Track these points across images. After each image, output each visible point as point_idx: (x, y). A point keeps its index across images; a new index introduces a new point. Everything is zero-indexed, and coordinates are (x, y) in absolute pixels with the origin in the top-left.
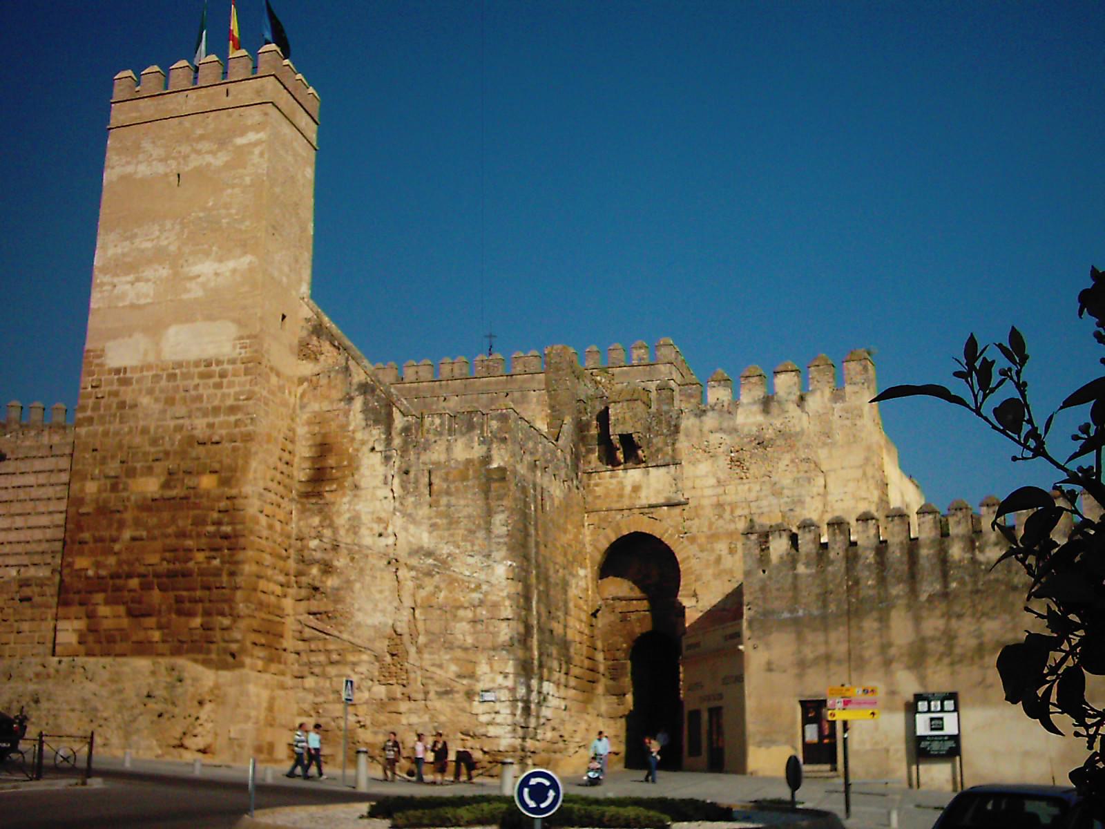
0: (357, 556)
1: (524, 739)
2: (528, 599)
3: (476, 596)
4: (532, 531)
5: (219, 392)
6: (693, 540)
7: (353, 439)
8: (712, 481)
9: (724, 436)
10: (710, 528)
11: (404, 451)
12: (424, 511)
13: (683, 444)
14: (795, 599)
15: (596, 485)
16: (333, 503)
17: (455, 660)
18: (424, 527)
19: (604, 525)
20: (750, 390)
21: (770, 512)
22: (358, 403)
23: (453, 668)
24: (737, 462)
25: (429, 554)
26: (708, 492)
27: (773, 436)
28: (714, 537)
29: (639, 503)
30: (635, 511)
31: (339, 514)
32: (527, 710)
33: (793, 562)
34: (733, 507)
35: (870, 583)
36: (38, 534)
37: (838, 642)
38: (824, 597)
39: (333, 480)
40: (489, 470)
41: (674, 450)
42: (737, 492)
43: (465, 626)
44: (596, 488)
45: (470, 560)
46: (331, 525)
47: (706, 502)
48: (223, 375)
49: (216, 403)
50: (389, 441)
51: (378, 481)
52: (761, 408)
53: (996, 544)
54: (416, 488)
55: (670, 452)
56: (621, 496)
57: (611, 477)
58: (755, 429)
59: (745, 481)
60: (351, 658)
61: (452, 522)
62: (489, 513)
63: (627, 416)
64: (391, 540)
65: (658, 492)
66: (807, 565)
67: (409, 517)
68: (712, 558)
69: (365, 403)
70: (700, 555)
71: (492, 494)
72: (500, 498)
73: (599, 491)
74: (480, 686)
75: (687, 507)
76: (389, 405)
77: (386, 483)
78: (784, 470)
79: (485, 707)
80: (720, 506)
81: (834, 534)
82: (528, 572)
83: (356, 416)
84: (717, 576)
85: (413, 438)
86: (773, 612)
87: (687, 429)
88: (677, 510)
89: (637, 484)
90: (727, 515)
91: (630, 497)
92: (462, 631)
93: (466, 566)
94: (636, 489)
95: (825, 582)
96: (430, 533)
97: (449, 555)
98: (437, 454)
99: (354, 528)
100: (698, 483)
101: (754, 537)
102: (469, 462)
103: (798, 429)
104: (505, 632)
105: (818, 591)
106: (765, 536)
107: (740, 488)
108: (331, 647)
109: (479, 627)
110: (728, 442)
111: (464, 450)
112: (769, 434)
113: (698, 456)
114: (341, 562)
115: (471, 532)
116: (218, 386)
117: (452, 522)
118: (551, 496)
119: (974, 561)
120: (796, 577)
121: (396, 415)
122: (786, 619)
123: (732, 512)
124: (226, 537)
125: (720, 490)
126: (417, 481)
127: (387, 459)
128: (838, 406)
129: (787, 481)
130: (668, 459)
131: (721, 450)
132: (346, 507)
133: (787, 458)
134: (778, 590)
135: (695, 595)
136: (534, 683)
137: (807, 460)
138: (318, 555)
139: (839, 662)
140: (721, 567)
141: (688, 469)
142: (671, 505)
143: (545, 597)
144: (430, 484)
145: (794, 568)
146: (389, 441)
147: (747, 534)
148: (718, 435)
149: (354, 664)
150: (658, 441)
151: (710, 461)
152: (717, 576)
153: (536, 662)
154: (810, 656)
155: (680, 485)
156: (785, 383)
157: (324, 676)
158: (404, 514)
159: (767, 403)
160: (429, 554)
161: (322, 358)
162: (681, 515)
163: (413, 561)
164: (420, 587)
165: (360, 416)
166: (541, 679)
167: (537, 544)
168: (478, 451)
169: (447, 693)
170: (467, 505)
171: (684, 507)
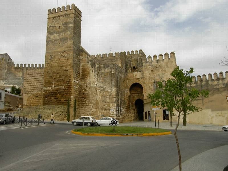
0: (90, 88)
1: (118, 117)
2: (118, 94)
3: (110, 94)
4: (119, 83)
5: (67, 62)
6: (145, 84)
7: (89, 69)
8: (148, 74)
11: (97, 71)
12: (101, 80)
13: (143, 68)
16: (86, 80)
17: (107, 104)
18: (101, 83)
21: (158, 79)
22: (90, 63)
23: (106, 106)
24: (152, 71)
25: (102, 87)
26: (148, 76)
28: (149, 83)
31: (87, 81)
32: (118, 112)
34: (152, 78)
36: (39, 86)
39: (86, 76)
40: (111, 74)
42: (153, 76)
43: (108, 99)
45: (109, 88)
46: (86, 83)
47: (148, 77)
48: (68, 59)
49: (67, 64)
50: (95, 69)
51: (93, 76)
53: (194, 84)
54: (100, 77)
56: (133, 77)
60: (90, 104)
61: (106, 82)
62: (111, 80)
64: (96, 85)
67: (98, 81)
69: (91, 63)
71: (112, 78)
72: (113, 78)
73: (130, 76)
74: (111, 108)
76: (95, 63)
77: (95, 76)
78: (160, 72)
79: (111, 112)
80: (150, 78)
82: (118, 90)
83: (90, 66)
84: (149, 90)
85: (99, 69)
88: (143, 79)
92: (108, 100)
93: (108, 89)
94: (136, 75)
96: (102, 84)
97: (105, 87)
98: (103, 71)
99: (90, 84)
100: (146, 74)
101: (155, 83)
102: (108, 72)
104: (115, 100)
108: (87, 103)
109: (110, 99)
111: (107, 70)
112: (158, 66)
114: (88, 89)
115: (108, 83)
116: (67, 61)
117: (106, 82)
118: (122, 77)
119: (191, 86)
121: (96, 65)
123: (152, 79)
124: (69, 86)
125: (150, 75)
126: (100, 75)
127: (95, 72)
128: (169, 61)
129: (161, 74)
133: (161, 70)
136: (120, 108)
137: (164, 70)
138: (84, 88)
142: (142, 78)
143: (121, 94)
144: (102, 76)
146: (95, 69)
147: (154, 82)
149: (90, 105)
150: (140, 68)
152: (149, 90)
153: (120, 105)
157: (86, 107)
158: (98, 81)
160: (102, 87)
161: (84, 56)
163: (99, 89)
164: (101, 93)
165: (90, 65)
166: (121, 107)
167: (119, 85)
168: (109, 70)
169: (105, 110)
170: (108, 79)
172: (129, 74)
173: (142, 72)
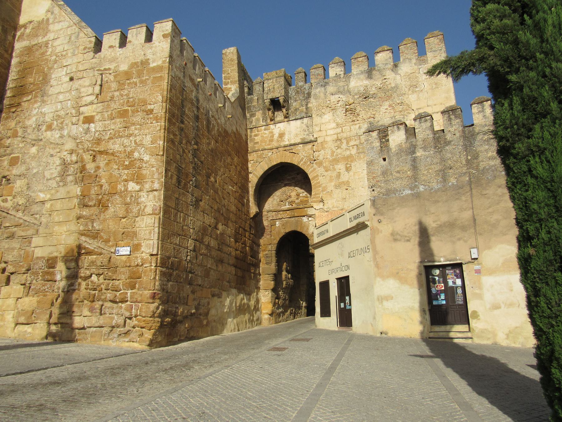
8: (334, 125)
9: (341, 96)
10: (332, 155)
13: (313, 103)
14: (415, 178)
15: (256, 135)
19: (260, 160)
20: (358, 66)
27: (376, 92)
28: (336, 161)
29: (282, 144)
30: (280, 149)
31: (29, 117)
33: (412, 149)
34: (348, 140)
35: (490, 154)
37: (462, 210)
38: (443, 174)
41: (307, 108)
44: (256, 138)
47: (328, 139)
52: (367, 75)
55: (305, 110)
57: (265, 130)
58: (362, 89)
59: (356, 122)
63: (276, 87)
65: (297, 135)
66: (425, 148)
68: (334, 174)
70: (326, 174)
73: (257, 139)
75: (315, 144)
80: (338, 139)
81: (450, 119)
84: (337, 187)
86: (395, 191)
87: (315, 95)
88: (310, 146)
89: (282, 132)
90: (344, 146)
91: (278, 141)
94: (281, 135)
95: (443, 160)
101: (375, 134)
103: (393, 85)
105: (438, 167)
106: (384, 134)
107: (352, 127)
110: (344, 99)
112: (373, 91)
113: (323, 111)
120: (414, 160)
122: (407, 195)
125: (339, 130)
130: (303, 115)
131: (339, 105)
132: (35, 112)
134: (398, 172)
135: (322, 201)
139: (464, 228)
140: (341, 180)
141: (316, 120)
145: (414, 152)
148: (337, 96)
151: (331, 113)
154: (434, 225)
155: (311, 130)
156: (383, 58)
159: (369, 73)
162: (312, 149)
171: (314, 143)
172: (255, 132)
173: (305, 120)
